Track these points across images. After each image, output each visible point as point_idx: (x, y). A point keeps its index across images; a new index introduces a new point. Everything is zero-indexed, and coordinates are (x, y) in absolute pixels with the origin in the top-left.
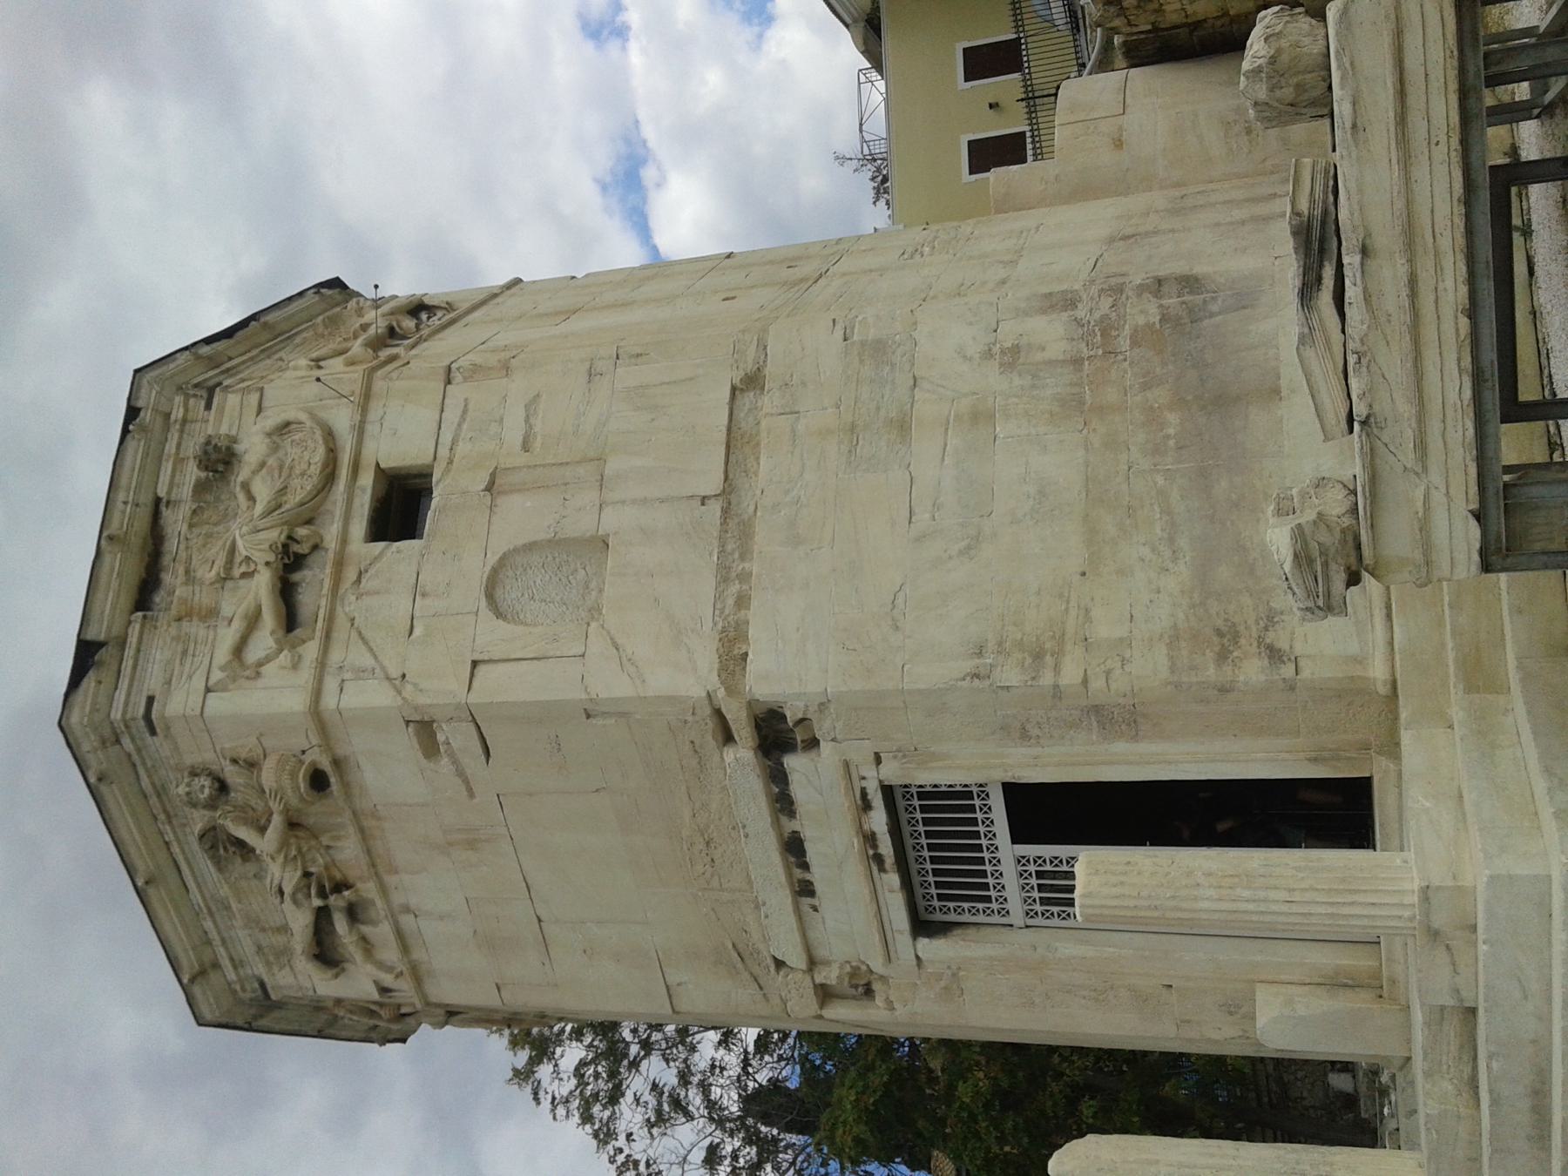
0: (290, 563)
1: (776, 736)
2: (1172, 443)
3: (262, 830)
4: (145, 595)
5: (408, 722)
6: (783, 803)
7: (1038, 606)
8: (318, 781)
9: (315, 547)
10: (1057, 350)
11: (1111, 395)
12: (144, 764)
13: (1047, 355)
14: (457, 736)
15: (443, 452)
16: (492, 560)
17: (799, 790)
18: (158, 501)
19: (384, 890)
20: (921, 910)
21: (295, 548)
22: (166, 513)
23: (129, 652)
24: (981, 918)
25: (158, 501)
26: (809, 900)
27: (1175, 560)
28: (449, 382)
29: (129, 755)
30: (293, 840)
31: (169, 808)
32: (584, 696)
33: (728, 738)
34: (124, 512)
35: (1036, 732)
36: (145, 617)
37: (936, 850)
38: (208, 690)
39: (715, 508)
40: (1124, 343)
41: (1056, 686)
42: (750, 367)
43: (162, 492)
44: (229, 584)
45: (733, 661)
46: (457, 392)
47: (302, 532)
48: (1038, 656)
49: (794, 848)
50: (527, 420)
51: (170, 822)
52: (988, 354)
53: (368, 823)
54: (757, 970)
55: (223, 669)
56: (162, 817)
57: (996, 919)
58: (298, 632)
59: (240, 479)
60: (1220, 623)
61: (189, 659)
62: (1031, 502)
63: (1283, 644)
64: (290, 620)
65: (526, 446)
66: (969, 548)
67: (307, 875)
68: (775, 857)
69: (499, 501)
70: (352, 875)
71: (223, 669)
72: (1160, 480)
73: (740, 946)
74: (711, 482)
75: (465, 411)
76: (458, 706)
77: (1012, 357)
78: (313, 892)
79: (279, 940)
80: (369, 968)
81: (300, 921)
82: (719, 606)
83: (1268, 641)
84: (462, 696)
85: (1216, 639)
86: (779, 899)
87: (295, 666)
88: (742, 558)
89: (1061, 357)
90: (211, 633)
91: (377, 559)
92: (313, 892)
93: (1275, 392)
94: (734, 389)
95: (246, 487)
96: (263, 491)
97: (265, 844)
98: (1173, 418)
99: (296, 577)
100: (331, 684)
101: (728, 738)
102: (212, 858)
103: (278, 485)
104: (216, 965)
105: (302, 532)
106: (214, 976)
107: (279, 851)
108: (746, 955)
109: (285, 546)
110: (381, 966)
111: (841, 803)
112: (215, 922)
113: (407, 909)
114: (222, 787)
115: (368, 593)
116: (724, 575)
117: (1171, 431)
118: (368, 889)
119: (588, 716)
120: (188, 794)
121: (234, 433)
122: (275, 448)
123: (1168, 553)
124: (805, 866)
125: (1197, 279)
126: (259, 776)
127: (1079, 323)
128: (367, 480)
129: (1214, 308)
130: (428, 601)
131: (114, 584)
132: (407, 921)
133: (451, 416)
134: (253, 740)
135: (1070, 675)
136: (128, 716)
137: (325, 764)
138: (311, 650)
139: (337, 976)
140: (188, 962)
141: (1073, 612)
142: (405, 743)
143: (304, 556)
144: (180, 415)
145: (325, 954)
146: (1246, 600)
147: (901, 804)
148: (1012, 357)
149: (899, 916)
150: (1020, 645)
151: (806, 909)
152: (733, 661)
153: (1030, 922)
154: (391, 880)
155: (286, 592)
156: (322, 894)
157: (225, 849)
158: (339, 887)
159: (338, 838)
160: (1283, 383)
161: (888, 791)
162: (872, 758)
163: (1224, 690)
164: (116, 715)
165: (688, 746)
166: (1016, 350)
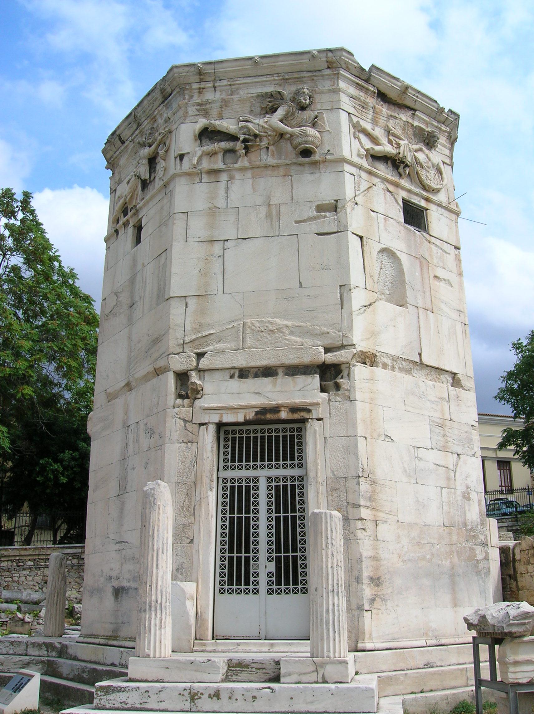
0: (395, 163)
1: (330, 374)
2: (440, 562)
4: (382, 96)
5: (337, 201)
6: (294, 370)
7: (387, 500)
8: (307, 153)
9: (401, 175)
11: (455, 538)
12: (316, 76)
14: (329, 222)
15: (433, 240)
16: (398, 254)
17: (301, 380)
18: (415, 110)
19: (242, 169)
20: (227, 428)
21: (402, 166)
22: (410, 113)
25: (415, 110)
26: (237, 375)
27: (403, 561)
29: (320, 71)
30: (275, 133)
31: (290, 81)
32: (352, 286)
33: (327, 350)
34: (414, 95)
35: (335, 495)
36: (375, 93)
37: (267, 440)
38: (349, 113)
39: (417, 360)
41: (360, 506)
42: (463, 383)
43: (417, 113)
44: (386, 133)
45: (368, 359)
46: (452, 250)
48: (370, 499)
49: (268, 372)
50: (444, 280)
51: (284, 79)
52: (468, 487)
53: (282, 171)
54: (197, 342)
55: (358, 122)
56: (287, 77)
57: (222, 464)
58: (370, 159)
59: (424, 149)
60: (382, 579)
61: (361, 108)
62: (421, 501)
63: (375, 605)
64: (375, 157)
65: (436, 277)
66: (406, 471)
67: (256, 136)
68: (264, 363)
70: (253, 156)
71: (358, 122)
72: (428, 557)
73: (211, 337)
74: (426, 361)
75: (446, 252)
76: (346, 226)
78: (247, 136)
79: (214, 112)
80: (199, 153)
81: (228, 125)
82: (385, 355)
83: (377, 599)
84: (350, 229)
85: (377, 577)
86: (241, 361)
87: (359, 155)
88: (399, 368)
89: (467, 518)
90: (369, 121)
91: (396, 201)
92: (247, 136)
93: (455, 605)
94: (455, 374)
95: (420, 150)
96: (421, 156)
97: (275, 120)
98: (447, 563)
99: (389, 162)
100: (353, 170)
101: (327, 350)
102: (266, 94)
103: (424, 165)
104: (201, 81)
106: (197, 78)
107: (269, 125)
108: (206, 339)
109: (403, 162)
110: (200, 159)
111: (298, 400)
112: (226, 85)
113: (231, 178)
114: (303, 108)
115: (385, 195)
116: (395, 359)
117: (444, 562)
118: (243, 162)
119: (341, 286)
120: (304, 93)
121: (437, 149)
122: (433, 166)
123: (405, 559)
124: (256, 376)
125: (489, 575)
126: (309, 126)
127: (477, 526)
128: (423, 203)
129: (481, 582)
130: (383, 221)
131: (390, 84)
132: (224, 177)
133: (446, 247)
134: (328, 129)
135: (364, 513)
136: (340, 76)
137: (316, 157)
138: (365, 163)
139: (195, 136)
141: (385, 516)
142: (327, 197)
143: (397, 169)
144: (443, 128)
145: (207, 134)
146: (390, 590)
147: (295, 426)
149: (228, 418)
150: (374, 492)
151: (232, 371)
152: (368, 359)
153: (221, 481)
154: (249, 174)
155: (384, 158)
156: (245, 141)
157: (270, 102)
158: (247, 148)
159: (273, 155)
160: (458, 609)
161: (304, 421)
162: (321, 417)
163: (358, 580)
164: (342, 72)
165: (325, 329)
166: (469, 499)
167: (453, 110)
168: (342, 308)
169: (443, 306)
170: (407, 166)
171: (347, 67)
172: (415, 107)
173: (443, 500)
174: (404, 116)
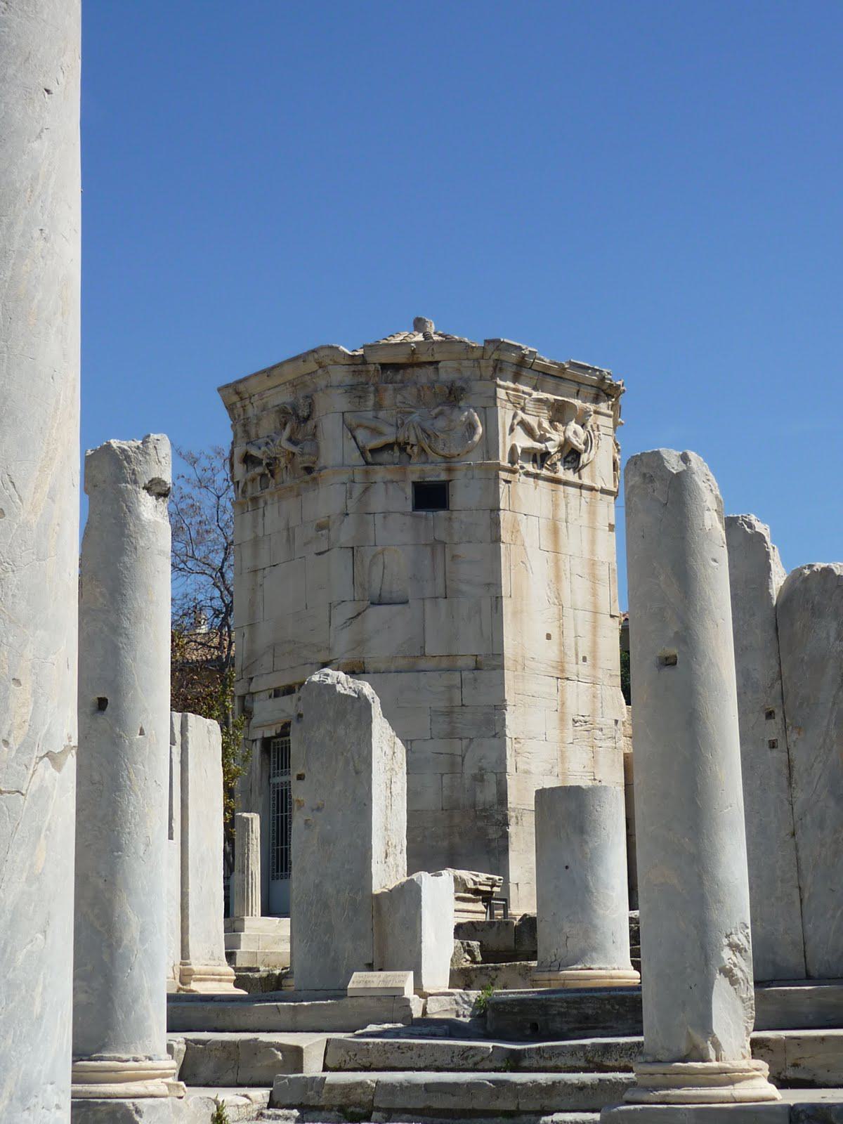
2: (434, 843)
3: (290, 440)
10: (480, 797)
13: (478, 793)
18: (439, 362)
21: (409, 447)
23: (360, 367)
24: (272, 766)
25: (437, 362)
28: (491, 510)
40: (480, 824)
43: (440, 365)
47: (416, 449)
52: (481, 769)
67: (275, 458)
69: (429, 549)
77: (479, 778)
98: (445, 843)
99: (396, 448)
105: (416, 449)
109: (408, 444)
128: (443, 477)
140: (241, 388)
148: (479, 778)
155: (388, 447)
166: (482, 780)
167: (488, 338)
168: (330, 625)
169: (464, 587)
170: (413, 445)
171: (335, 362)
172: (437, 358)
173: (444, 785)
174: (424, 375)
